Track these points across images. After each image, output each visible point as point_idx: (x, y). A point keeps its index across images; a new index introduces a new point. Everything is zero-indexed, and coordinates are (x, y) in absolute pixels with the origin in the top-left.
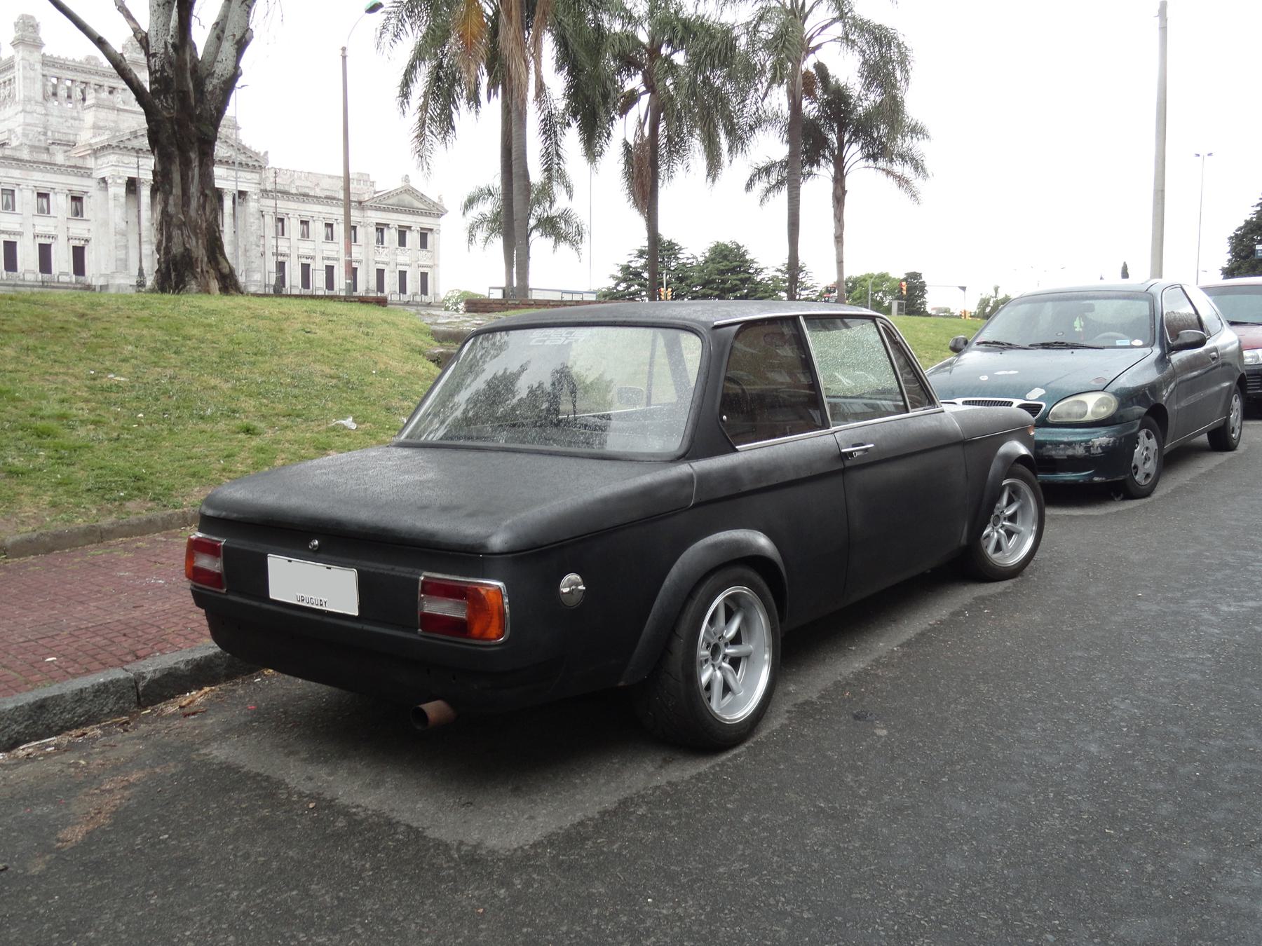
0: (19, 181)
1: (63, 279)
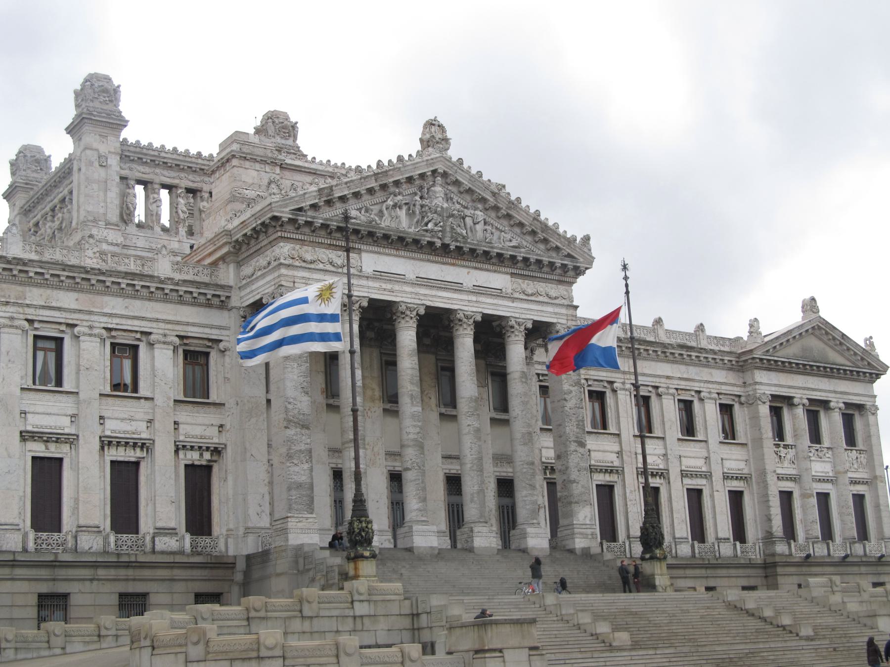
0: (72, 318)
1: (165, 543)
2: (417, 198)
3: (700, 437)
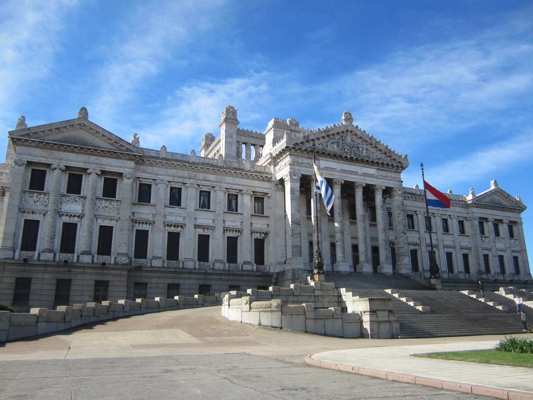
0: (214, 184)
1: (247, 267)
2: (341, 140)
3: (451, 232)
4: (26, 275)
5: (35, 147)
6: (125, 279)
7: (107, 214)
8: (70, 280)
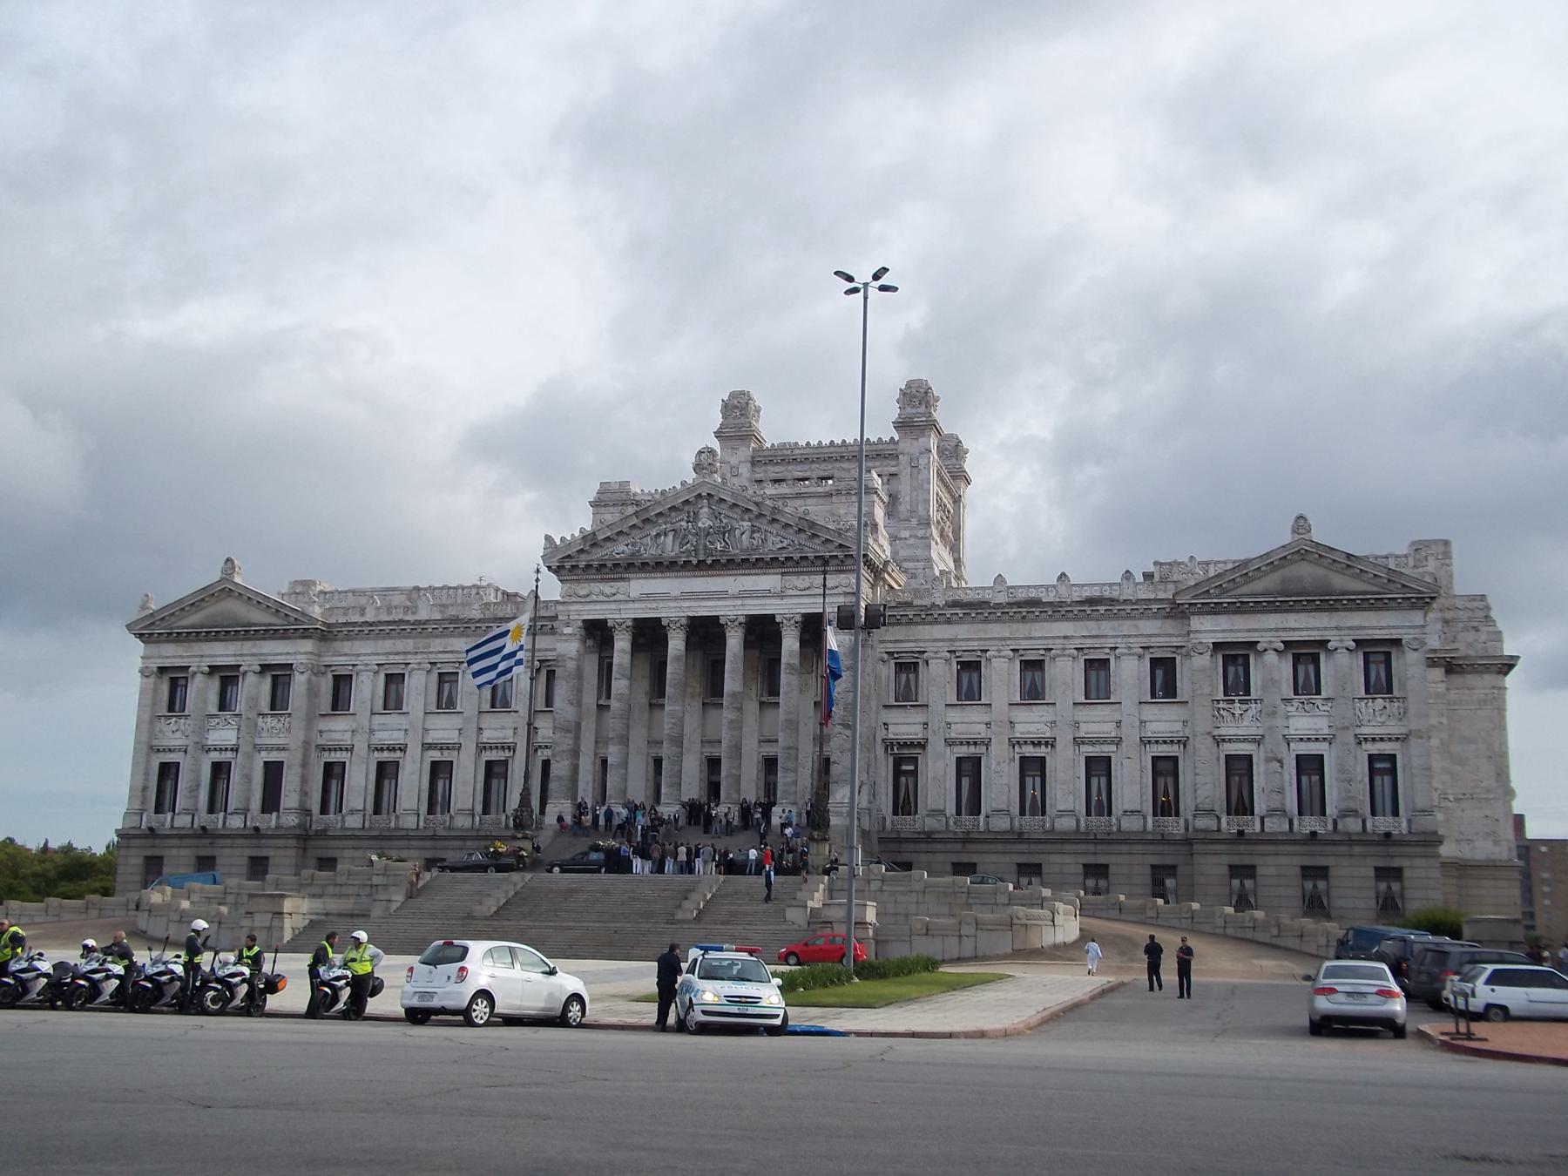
4: (156, 852)
5: (167, 641)
6: (292, 852)
7: (274, 741)
8: (214, 858)
